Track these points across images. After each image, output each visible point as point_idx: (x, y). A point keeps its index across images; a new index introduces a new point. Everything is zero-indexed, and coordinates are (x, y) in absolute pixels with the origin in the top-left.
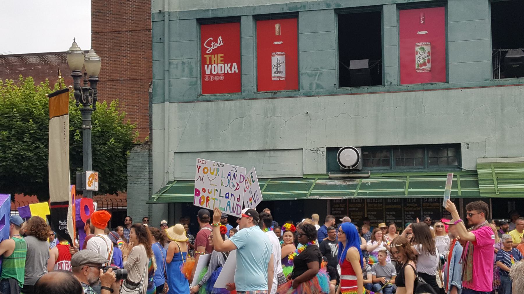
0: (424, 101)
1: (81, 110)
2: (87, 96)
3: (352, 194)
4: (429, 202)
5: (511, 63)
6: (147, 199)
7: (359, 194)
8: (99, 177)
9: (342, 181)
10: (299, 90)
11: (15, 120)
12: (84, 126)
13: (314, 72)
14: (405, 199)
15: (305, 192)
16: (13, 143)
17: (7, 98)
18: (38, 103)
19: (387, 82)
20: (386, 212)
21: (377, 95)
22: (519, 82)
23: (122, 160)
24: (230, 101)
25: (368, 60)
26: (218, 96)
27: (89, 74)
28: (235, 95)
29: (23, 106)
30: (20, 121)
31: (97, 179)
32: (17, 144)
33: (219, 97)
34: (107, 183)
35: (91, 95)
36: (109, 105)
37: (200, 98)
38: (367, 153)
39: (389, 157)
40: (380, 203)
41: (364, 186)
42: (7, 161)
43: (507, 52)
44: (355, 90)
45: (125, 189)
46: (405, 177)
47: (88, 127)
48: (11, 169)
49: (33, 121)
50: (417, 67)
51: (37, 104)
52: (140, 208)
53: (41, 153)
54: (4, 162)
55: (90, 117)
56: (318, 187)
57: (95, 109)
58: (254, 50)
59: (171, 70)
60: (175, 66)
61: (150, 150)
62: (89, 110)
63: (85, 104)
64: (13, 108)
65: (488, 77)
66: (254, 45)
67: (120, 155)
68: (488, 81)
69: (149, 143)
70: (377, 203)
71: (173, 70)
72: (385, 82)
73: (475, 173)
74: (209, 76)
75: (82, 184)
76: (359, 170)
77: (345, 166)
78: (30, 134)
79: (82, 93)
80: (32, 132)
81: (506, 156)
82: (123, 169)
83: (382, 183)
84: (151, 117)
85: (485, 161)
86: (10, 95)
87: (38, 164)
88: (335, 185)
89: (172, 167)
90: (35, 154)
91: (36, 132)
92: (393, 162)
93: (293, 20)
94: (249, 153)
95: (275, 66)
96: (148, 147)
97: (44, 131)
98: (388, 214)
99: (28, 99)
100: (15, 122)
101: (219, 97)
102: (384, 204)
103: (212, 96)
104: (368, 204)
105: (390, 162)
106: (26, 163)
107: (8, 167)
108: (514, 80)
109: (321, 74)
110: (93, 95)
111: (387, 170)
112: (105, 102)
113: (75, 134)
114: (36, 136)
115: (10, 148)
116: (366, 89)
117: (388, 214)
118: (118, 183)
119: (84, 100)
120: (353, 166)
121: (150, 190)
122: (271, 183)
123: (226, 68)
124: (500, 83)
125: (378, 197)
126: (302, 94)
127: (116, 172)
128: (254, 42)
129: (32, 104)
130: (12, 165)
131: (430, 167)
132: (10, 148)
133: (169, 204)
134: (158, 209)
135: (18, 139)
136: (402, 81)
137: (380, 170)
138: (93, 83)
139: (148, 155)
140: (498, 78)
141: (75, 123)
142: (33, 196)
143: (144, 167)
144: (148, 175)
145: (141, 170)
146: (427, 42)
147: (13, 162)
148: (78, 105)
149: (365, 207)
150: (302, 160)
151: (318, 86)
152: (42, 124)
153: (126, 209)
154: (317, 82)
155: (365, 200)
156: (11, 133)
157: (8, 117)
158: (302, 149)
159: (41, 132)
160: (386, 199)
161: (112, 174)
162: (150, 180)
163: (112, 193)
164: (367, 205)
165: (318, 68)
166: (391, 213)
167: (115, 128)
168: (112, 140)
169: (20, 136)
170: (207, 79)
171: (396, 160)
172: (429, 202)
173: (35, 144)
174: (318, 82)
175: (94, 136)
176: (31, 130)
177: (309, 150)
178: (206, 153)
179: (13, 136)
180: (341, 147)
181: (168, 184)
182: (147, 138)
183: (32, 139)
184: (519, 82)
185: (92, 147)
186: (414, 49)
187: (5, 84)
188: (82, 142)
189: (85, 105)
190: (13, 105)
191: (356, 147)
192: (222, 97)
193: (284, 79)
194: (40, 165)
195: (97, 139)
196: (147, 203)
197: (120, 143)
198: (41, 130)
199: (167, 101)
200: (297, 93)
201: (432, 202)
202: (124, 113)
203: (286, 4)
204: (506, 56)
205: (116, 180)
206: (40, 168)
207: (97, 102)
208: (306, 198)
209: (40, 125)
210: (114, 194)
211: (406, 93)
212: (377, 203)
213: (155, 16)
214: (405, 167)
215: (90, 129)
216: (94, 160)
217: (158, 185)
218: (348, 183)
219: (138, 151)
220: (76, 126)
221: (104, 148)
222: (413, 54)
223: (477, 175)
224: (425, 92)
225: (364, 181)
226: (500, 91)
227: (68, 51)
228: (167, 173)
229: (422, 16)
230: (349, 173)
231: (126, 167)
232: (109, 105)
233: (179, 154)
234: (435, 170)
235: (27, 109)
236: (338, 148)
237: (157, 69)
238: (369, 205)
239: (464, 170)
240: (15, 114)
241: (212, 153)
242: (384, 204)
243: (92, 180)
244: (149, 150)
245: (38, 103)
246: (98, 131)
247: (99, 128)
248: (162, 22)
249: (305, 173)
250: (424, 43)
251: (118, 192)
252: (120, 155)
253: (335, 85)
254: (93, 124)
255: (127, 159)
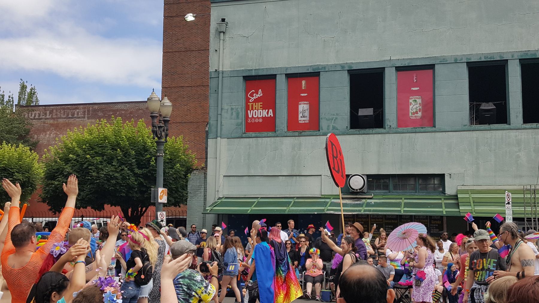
0: (416, 140)
1: (156, 142)
2: (161, 131)
3: (360, 211)
4: (419, 219)
5: (484, 113)
6: (202, 211)
7: (365, 211)
8: (168, 193)
9: (352, 200)
10: (319, 131)
11: (106, 149)
12: (158, 154)
13: (331, 117)
14: (401, 216)
15: (323, 208)
16: (105, 166)
17: (101, 133)
18: (124, 137)
19: (387, 126)
20: (385, 225)
21: (380, 135)
22: (490, 128)
23: (184, 180)
24: (266, 138)
25: (373, 109)
26: (257, 134)
27: (164, 115)
28: (270, 134)
29: (113, 138)
30: (110, 150)
31: (167, 194)
32: (107, 167)
33: (258, 135)
34: (173, 197)
35: (164, 131)
36: (176, 138)
37: (244, 135)
38: (371, 180)
39: (388, 183)
40: (381, 218)
41: (368, 205)
42: (99, 179)
43: (480, 105)
44: (362, 131)
45: (186, 203)
46: (401, 199)
47: (161, 155)
48: (103, 185)
49: (120, 150)
50: (410, 115)
51: (123, 137)
52: (196, 218)
53: (125, 174)
54: (97, 180)
55: (162, 148)
56: (333, 204)
57: (166, 142)
58: (286, 100)
59: (223, 114)
60: (226, 111)
61: (205, 174)
62: (162, 142)
63: (159, 137)
64: (105, 140)
65: (466, 124)
66: (286, 96)
67: (183, 176)
68: (466, 127)
69: (204, 168)
70: (378, 218)
71: (224, 114)
72: (386, 125)
73: (456, 197)
74: (251, 119)
75: (155, 198)
76: (364, 193)
77: (354, 189)
78: (118, 160)
79: (157, 129)
80: (119, 158)
81: (480, 184)
82: (185, 187)
83: (383, 202)
84: (207, 148)
85: (463, 188)
86: (104, 130)
87: (122, 182)
88: (346, 203)
89: (222, 187)
90: (121, 175)
91: (122, 158)
92: (391, 187)
93: (316, 77)
94: (280, 177)
95: (301, 112)
96: (204, 171)
97: (128, 158)
98: (387, 227)
99: (117, 134)
100: (106, 150)
101: (258, 135)
102: (384, 219)
103: (253, 134)
104: (372, 219)
105: (389, 187)
106: (113, 182)
107: (100, 184)
108: (486, 126)
109: (336, 118)
110: (165, 131)
111: (386, 193)
112: (173, 138)
113: (151, 161)
114: (122, 161)
115: (102, 170)
116: (371, 131)
117: (387, 227)
118: (181, 198)
119: (159, 135)
120: (360, 189)
121: (205, 204)
122: (297, 200)
123: (264, 113)
124: (475, 128)
125: (380, 213)
126: (321, 134)
127: (180, 190)
128: (286, 94)
129: (120, 138)
130: (103, 183)
131: (421, 191)
132: (102, 170)
133: (218, 214)
134: (211, 219)
135: (108, 163)
136: (399, 126)
137: (381, 193)
138: (166, 122)
139: (204, 178)
140: (473, 125)
141: (151, 153)
142: (117, 206)
143: (201, 187)
144: (203, 192)
145: (199, 189)
146: (418, 96)
147: (105, 180)
148: (154, 138)
149: (368, 221)
150: (320, 183)
151: (334, 128)
152: (126, 153)
153: (186, 218)
154: (333, 124)
155: (369, 215)
156: (103, 159)
157: (102, 147)
158: (321, 175)
159: (126, 159)
160: (385, 215)
161: (177, 191)
162: (205, 196)
163: (175, 206)
164: (371, 220)
165: (334, 114)
166: (390, 226)
167: (181, 156)
168: (178, 165)
169: (110, 161)
170: (249, 121)
171: (394, 186)
172: (419, 219)
173: (121, 167)
174: (334, 125)
175: (165, 162)
176: (118, 157)
177: (326, 176)
178: (247, 177)
179: (104, 161)
180: (351, 175)
181: (218, 200)
182: (203, 165)
183: (119, 163)
184: (490, 128)
185: (164, 170)
186: (409, 101)
187: (100, 123)
188: (156, 167)
189: (159, 138)
190: (106, 138)
191: (362, 175)
192: (261, 135)
193: (308, 122)
194: (124, 183)
195: (166, 164)
196: (202, 214)
197: (183, 167)
198: (126, 157)
199: (219, 137)
200: (317, 132)
201: (422, 219)
202: (187, 146)
203: (311, 66)
204: (482, 108)
205: (180, 196)
206: (124, 185)
207: (168, 138)
208: (324, 213)
209: (125, 153)
210: (178, 207)
211: (402, 134)
212: (378, 218)
213: (212, 74)
214: (401, 191)
215: (162, 156)
216: (164, 180)
217: (211, 200)
218: (356, 202)
219: (196, 174)
220: (152, 154)
221: (172, 171)
222: (408, 104)
223: (458, 198)
224: (417, 134)
225: (369, 201)
226: (475, 134)
227: (148, 99)
228: (218, 191)
229: (415, 77)
230: (356, 195)
231: (187, 186)
232: (176, 138)
233: (228, 177)
234: (424, 194)
235: (116, 141)
236: (349, 175)
237: (212, 113)
238: (372, 219)
239: (447, 195)
240: (106, 144)
241: (252, 177)
242: (384, 219)
243: (163, 194)
244: (205, 174)
245: (124, 137)
246: (168, 159)
247: (168, 156)
248: (218, 78)
249: (322, 194)
250: (416, 97)
251: (181, 205)
252: (183, 176)
253: (347, 127)
254: (164, 153)
255: (189, 180)
